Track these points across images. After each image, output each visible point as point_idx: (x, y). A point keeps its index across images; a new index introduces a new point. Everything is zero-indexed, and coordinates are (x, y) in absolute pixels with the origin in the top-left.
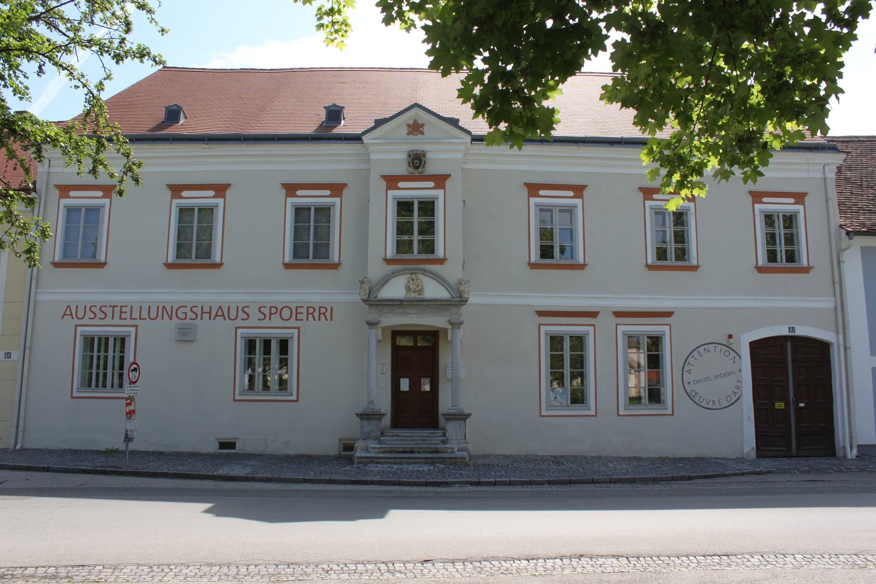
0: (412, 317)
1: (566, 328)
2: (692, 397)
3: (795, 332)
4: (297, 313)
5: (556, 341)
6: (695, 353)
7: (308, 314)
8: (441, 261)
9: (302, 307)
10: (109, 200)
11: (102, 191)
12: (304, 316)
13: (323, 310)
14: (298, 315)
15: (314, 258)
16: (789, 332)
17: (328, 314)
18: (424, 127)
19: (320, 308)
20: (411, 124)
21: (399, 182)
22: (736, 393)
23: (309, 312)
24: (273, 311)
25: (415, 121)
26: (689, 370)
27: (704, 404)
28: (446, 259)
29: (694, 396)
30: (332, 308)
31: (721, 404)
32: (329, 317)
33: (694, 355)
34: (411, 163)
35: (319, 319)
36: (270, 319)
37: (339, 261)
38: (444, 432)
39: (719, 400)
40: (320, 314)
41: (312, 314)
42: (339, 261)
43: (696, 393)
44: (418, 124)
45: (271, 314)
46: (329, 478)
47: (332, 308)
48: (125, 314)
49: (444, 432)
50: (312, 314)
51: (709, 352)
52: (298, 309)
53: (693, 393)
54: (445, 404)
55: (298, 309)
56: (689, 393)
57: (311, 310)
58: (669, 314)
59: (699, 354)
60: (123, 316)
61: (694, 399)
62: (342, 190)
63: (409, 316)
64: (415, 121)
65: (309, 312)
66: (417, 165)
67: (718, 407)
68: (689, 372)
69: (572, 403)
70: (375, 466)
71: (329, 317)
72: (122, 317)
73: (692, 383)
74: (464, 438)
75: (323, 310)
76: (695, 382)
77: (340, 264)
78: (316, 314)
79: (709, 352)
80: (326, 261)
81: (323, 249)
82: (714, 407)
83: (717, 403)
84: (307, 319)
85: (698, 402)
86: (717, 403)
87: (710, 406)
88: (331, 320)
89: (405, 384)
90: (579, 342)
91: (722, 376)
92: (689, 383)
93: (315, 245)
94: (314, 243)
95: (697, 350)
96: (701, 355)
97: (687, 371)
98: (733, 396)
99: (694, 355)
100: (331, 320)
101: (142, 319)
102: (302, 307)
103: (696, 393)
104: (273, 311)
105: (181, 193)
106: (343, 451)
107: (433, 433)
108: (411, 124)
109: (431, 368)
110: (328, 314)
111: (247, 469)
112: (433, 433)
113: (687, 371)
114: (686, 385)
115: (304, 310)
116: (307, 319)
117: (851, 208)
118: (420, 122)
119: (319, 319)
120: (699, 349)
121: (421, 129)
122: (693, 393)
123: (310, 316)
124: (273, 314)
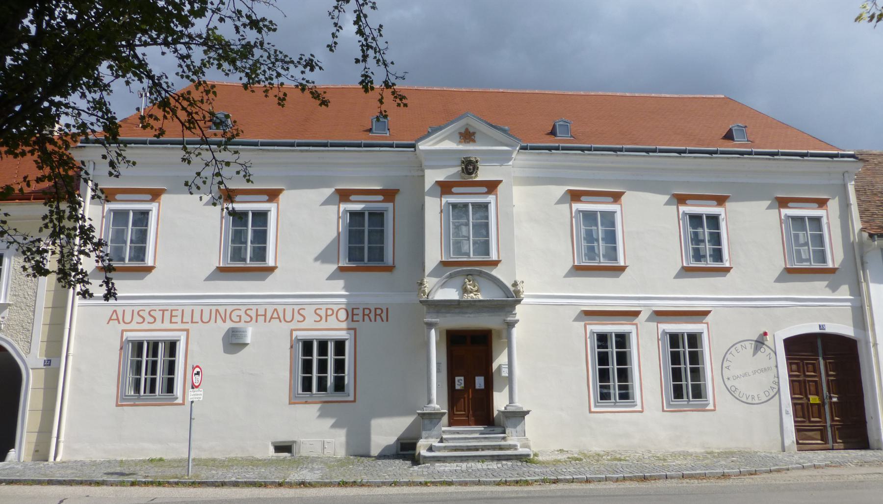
0: (469, 317)
1: (612, 328)
2: (732, 392)
3: (825, 329)
4: (353, 315)
5: (602, 339)
6: (733, 349)
7: (364, 315)
8: (495, 263)
9: (358, 309)
10: (392, 204)
11: (267, 195)
12: (360, 318)
13: (379, 312)
14: (354, 316)
15: (369, 260)
16: (820, 329)
17: (384, 315)
18: (476, 135)
19: (376, 309)
20: (463, 132)
21: (453, 187)
22: (774, 388)
23: (365, 313)
24: (330, 312)
25: (467, 129)
26: (728, 366)
27: (744, 399)
28: (500, 261)
29: (734, 392)
30: (387, 309)
31: (760, 399)
32: (384, 318)
33: (731, 352)
34: (465, 170)
35: (375, 321)
36: (326, 321)
37: (394, 263)
38: (503, 429)
39: (758, 395)
40: (376, 315)
41: (368, 315)
42: (394, 263)
43: (736, 389)
44: (470, 132)
45: (327, 316)
46: (408, 480)
47: (387, 309)
48: (357, 316)
49: (503, 429)
50: (368, 315)
51: (746, 348)
52: (355, 310)
53: (733, 389)
54: (500, 402)
55: (355, 310)
56: (729, 389)
57: (367, 312)
58: (706, 313)
59: (737, 351)
60: (355, 318)
61: (734, 394)
62: (395, 196)
63: (467, 315)
64: (467, 129)
65: (365, 313)
66: (471, 171)
67: (757, 401)
68: (728, 368)
69: (601, 399)
70: (444, 466)
71: (384, 318)
72: (354, 320)
73: (731, 379)
74: (523, 435)
75: (379, 312)
76: (735, 378)
77: (395, 266)
78: (372, 316)
79: (746, 348)
80: (381, 264)
81: (378, 254)
82: (754, 402)
83: (756, 398)
84: (364, 320)
85: (738, 397)
86: (756, 398)
87: (750, 401)
88: (387, 320)
89: (480, 382)
90: (622, 340)
91: (759, 371)
92: (728, 379)
93: (369, 248)
94: (364, 243)
95: (735, 347)
96: (738, 351)
97: (726, 367)
98: (771, 391)
99: (731, 352)
100: (387, 320)
101: (355, 321)
102: (358, 309)
103: (736, 389)
104: (330, 312)
105: (349, 197)
106: (401, 451)
107: (493, 430)
108: (463, 132)
109: (485, 366)
110: (384, 315)
111: (316, 473)
112: (493, 430)
113: (726, 367)
114: (726, 380)
115: (360, 312)
116: (364, 320)
117: (866, 213)
118: (471, 130)
119: (375, 321)
120: (736, 346)
121: (473, 137)
122: (733, 389)
123: (366, 318)
124: (329, 316)
